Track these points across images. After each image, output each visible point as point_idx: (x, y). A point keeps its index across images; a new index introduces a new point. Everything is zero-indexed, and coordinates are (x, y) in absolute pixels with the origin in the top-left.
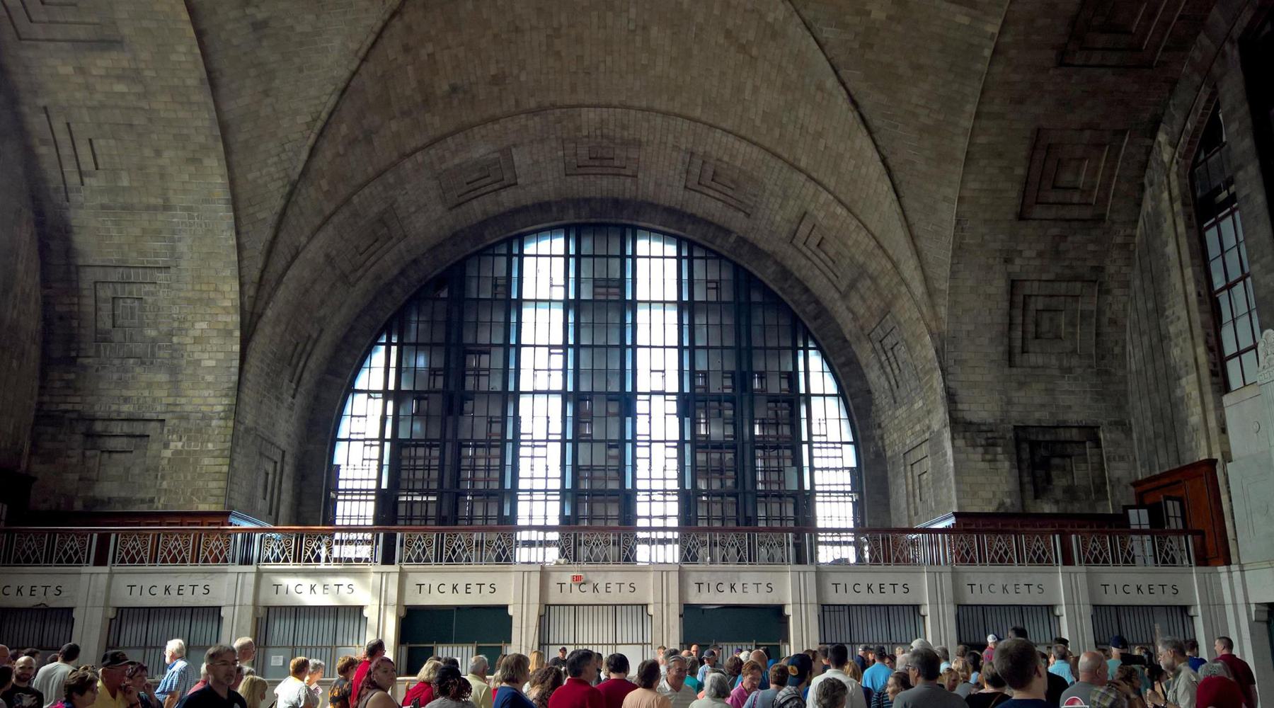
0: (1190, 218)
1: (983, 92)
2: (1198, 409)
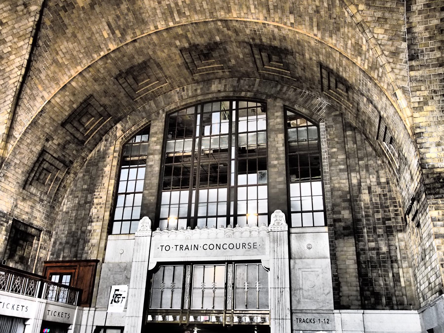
0: (119, 161)
1: (89, 67)
2: (98, 238)
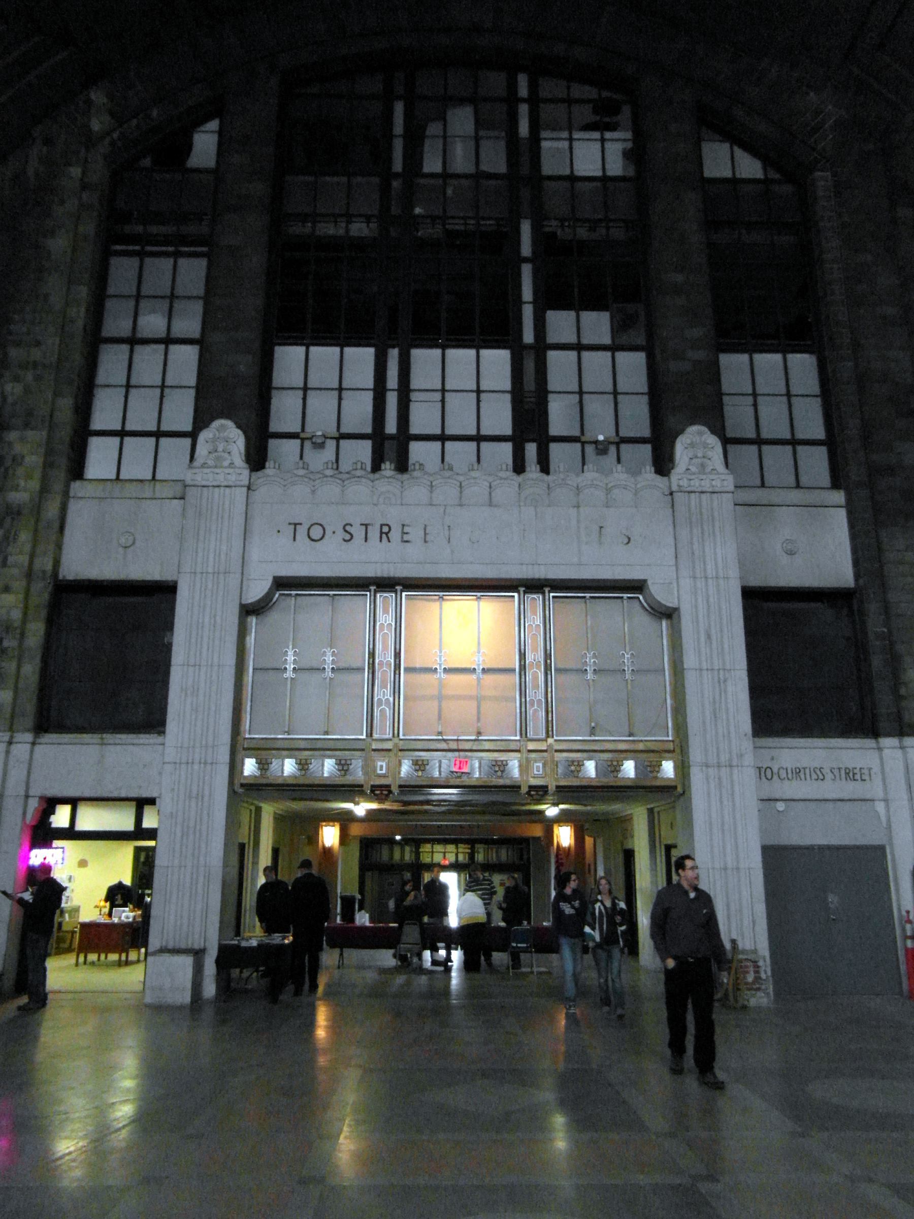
2: (34, 484)
